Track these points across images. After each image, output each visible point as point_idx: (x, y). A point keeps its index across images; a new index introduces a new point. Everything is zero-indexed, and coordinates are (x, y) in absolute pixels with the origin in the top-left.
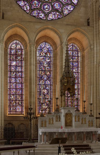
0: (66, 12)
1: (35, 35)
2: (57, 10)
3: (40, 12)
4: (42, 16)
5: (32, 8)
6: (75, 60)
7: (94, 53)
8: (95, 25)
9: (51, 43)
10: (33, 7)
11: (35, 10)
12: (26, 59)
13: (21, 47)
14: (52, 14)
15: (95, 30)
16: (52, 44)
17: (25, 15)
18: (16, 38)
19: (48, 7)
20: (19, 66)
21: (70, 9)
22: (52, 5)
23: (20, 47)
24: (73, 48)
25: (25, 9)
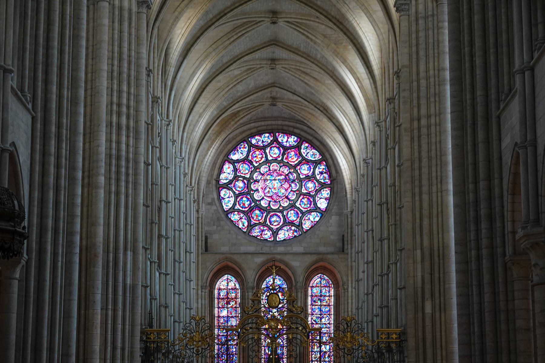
0: (307, 225)
1: (254, 273)
2: (292, 223)
3: (264, 229)
4: (267, 235)
5: (252, 223)
6: (325, 302)
7: (348, 296)
8: (349, 250)
9: (283, 276)
10: (253, 222)
11: (256, 226)
12: (243, 306)
13: (235, 285)
14: (283, 231)
15: (349, 260)
16: (285, 278)
17: (241, 236)
18: (227, 272)
19: (278, 219)
20: (232, 317)
21: (314, 219)
22: (285, 216)
23: (233, 285)
24: (321, 282)
25: (241, 226)
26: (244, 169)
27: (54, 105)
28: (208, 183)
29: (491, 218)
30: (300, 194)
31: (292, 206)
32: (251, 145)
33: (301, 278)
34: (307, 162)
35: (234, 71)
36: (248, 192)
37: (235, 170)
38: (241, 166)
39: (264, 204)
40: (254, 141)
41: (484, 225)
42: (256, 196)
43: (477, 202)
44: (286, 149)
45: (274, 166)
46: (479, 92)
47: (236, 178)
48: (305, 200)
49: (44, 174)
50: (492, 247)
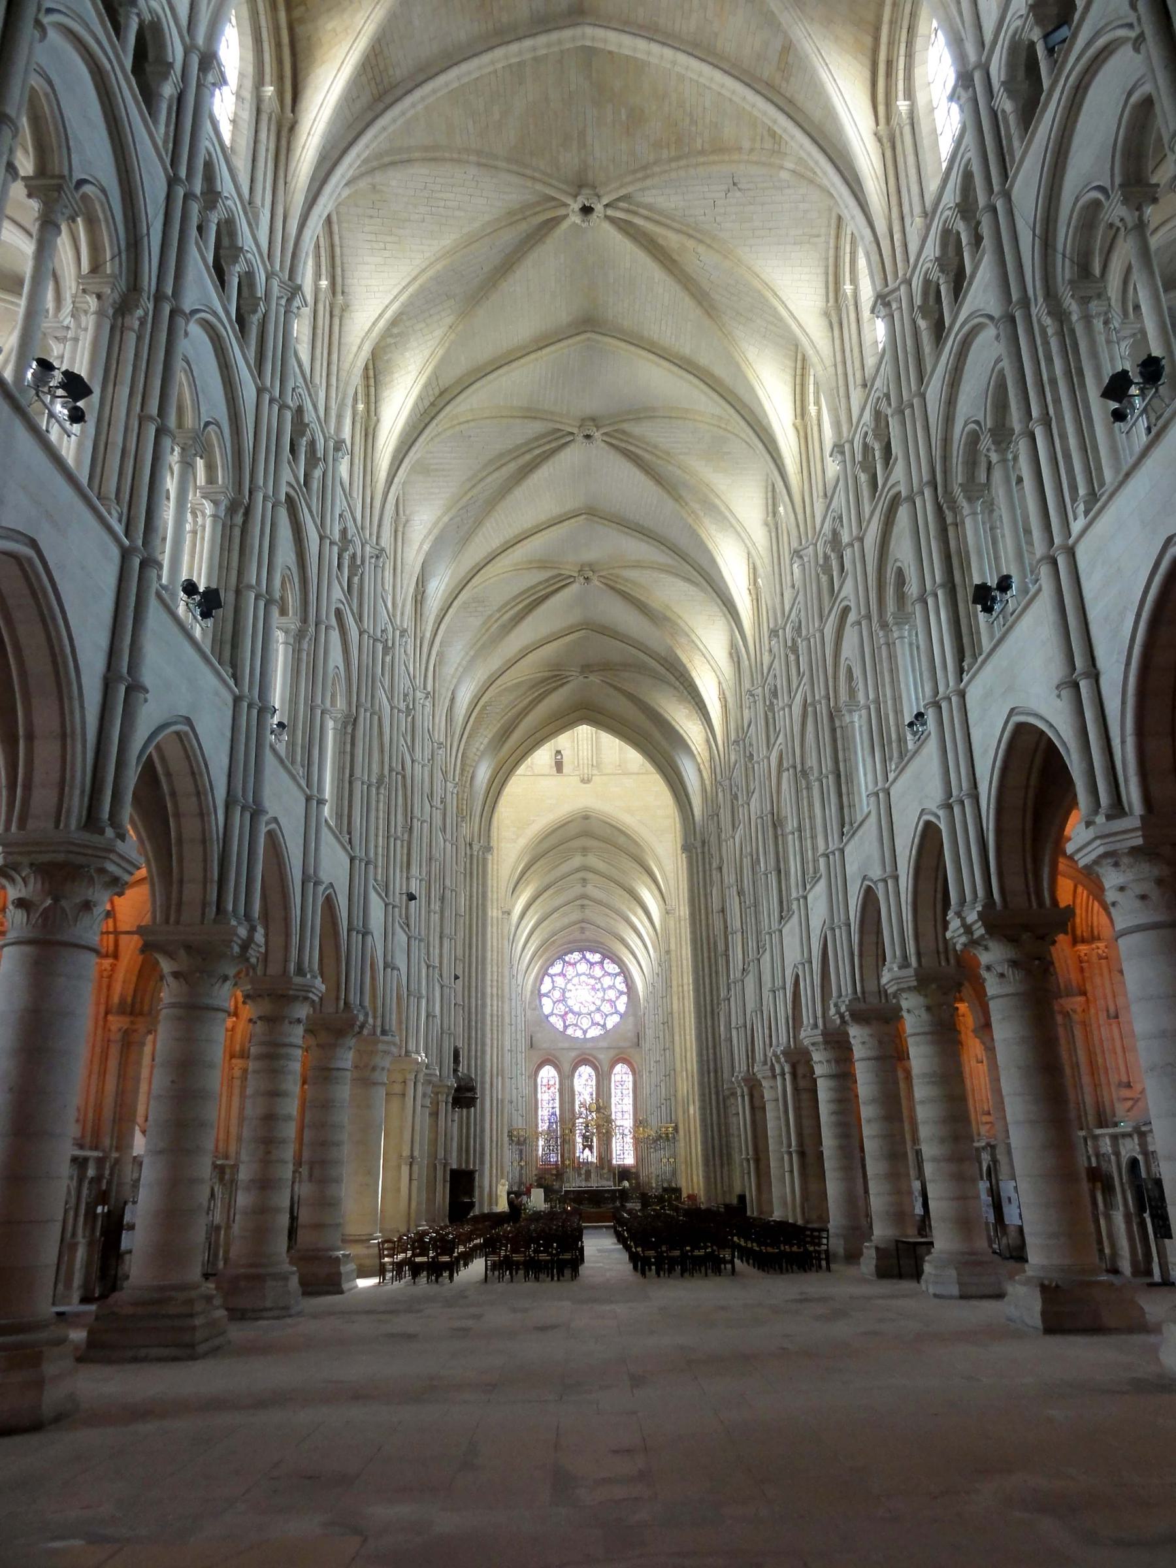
0: (609, 1026)
2: (598, 1024)
4: (579, 1034)
26: (560, 981)
27: (473, 1010)
28: (532, 992)
29: (716, 1072)
30: (603, 1000)
31: (598, 1010)
32: (564, 962)
33: (606, 1068)
34: (609, 974)
35: (555, 915)
36: (563, 1000)
37: (553, 982)
38: (555, 979)
39: (576, 1009)
40: (567, 958)
41: (712, 1075)
42: (570, 1002)
43: (708, 1061)
44: (592, 964)
45: (583, 978)
46: (708, 998)
47: (554, 988)
48: (608, 1005)
49: (469, 1051)
50: (716, 1086)
